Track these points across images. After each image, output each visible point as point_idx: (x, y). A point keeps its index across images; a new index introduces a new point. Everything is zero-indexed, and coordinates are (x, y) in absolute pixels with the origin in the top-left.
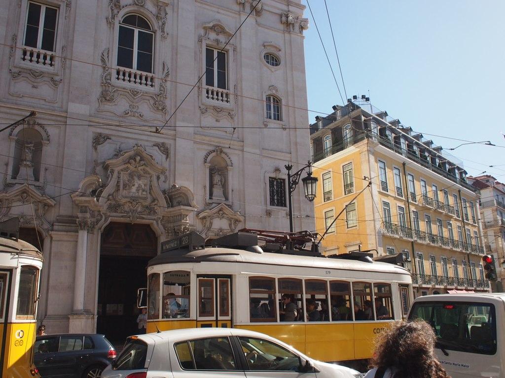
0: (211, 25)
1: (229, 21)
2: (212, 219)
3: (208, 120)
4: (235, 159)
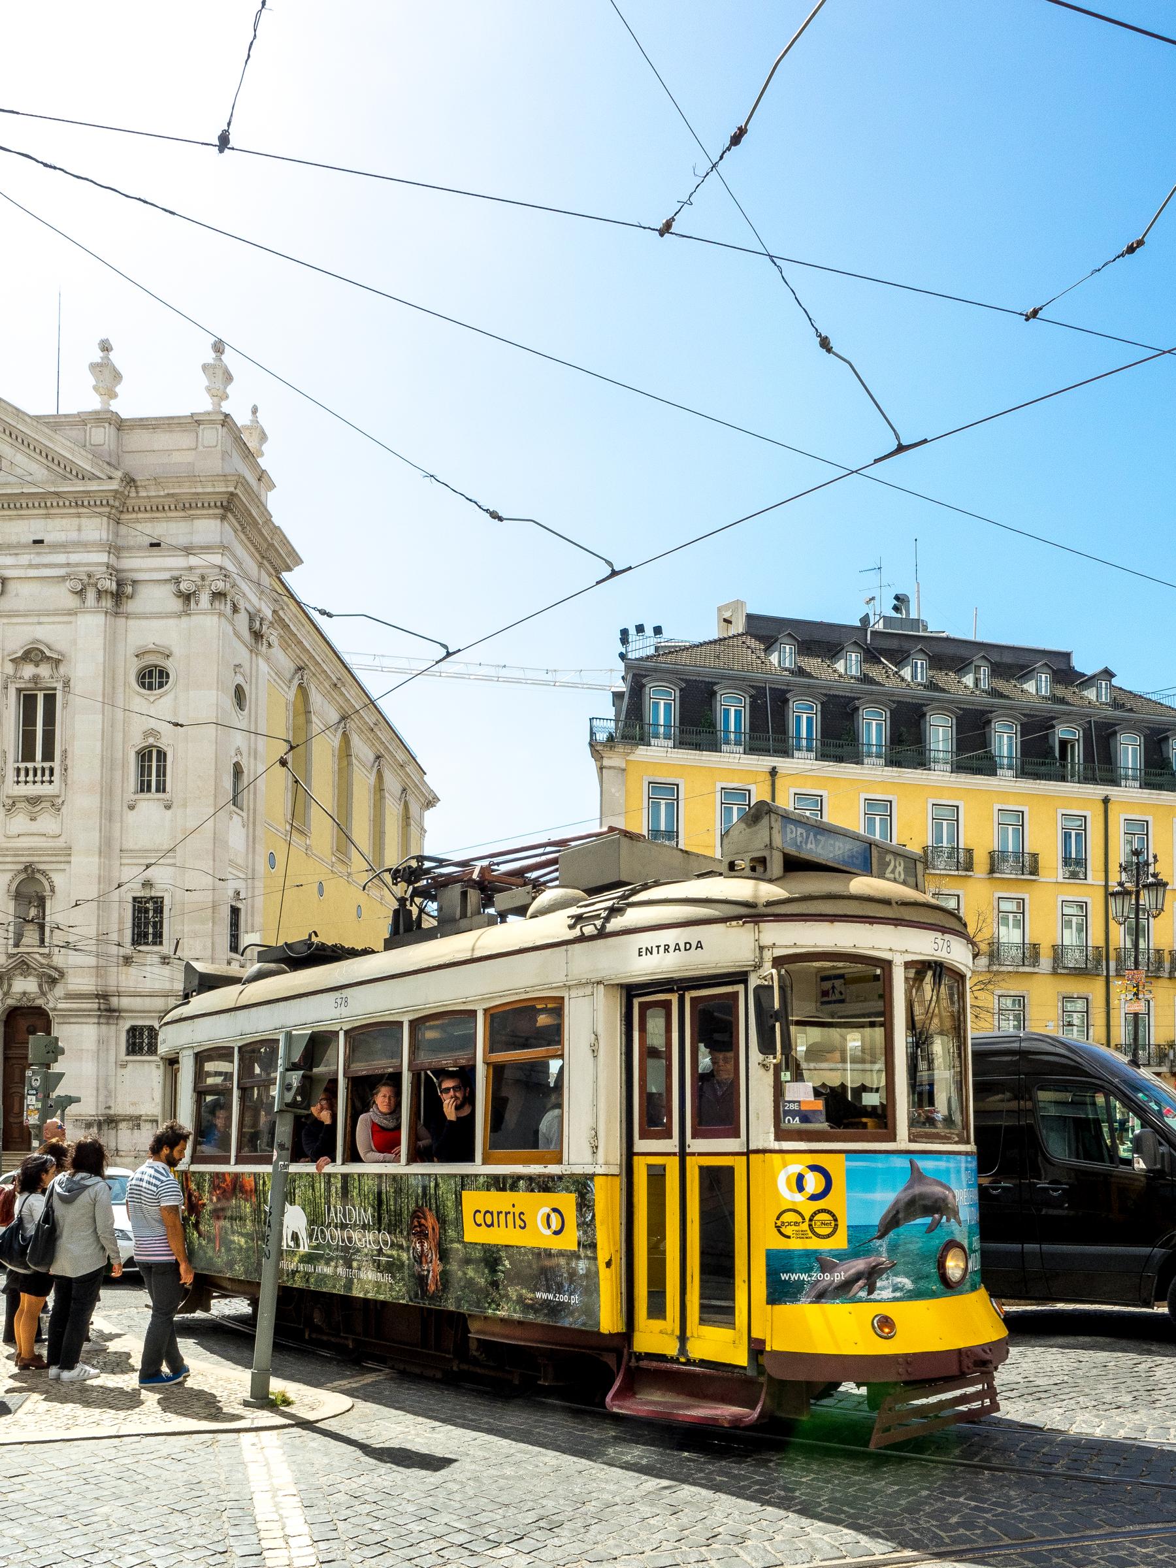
0: (19, 654)
1: (50, 634)
2: (10, 979)
3: (20, 822)
4: (57, 879)
